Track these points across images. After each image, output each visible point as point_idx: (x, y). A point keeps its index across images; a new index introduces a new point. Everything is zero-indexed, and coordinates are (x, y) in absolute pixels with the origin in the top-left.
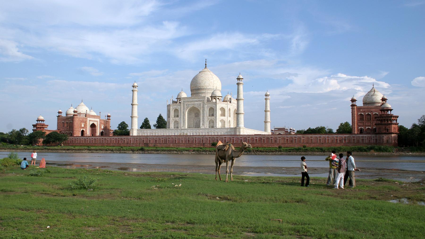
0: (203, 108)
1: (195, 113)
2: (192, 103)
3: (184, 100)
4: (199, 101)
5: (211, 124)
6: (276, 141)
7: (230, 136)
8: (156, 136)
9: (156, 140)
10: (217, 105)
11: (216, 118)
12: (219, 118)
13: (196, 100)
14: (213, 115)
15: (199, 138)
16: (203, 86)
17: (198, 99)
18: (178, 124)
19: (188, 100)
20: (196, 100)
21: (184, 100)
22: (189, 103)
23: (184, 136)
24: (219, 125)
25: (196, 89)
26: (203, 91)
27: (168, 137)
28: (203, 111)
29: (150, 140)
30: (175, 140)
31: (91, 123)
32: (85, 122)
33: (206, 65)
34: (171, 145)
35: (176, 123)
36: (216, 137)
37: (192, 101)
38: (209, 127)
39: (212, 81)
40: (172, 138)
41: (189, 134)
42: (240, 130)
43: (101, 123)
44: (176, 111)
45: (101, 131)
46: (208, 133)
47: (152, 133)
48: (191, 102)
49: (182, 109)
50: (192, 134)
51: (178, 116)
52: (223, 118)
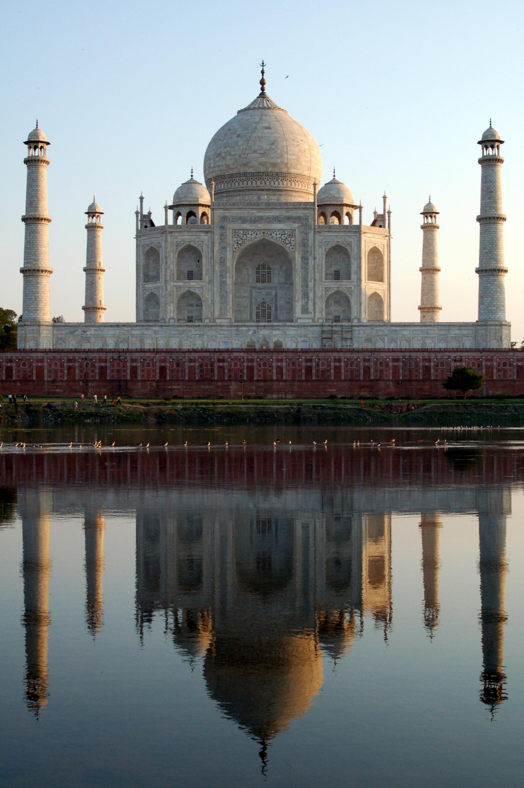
0: (305, 244)
1: (266, 260)
2: (260, 226)
3: (227, 213)
4: (288, 218)
5: (335, 310)
7: (477, 355)
8: (162, 351)
9: (163, 369)
10: (364, 238)
11: (359, 285)
12: (369, 287)
13: (275, 213)
14: (337, 276)
15: (350, 362)
16: (274, 165)
17: (284, 213)
18: (200, 305)
19: (244, 213)
20: (275, 213)
22: (247, 226)
23: (268, 351)
25: (245, 174)
26: (275, 184)
27: (216, 356)
28: (305, 259)
29: (134, 370)
30: (251, 369)
33: (262, 82)
34: (233, 386)
35: (191, 301)
36: (420, 355)
37: (260, 219)
39: (307, 147)
40: (237, 358)
41: (289, 345)
42: (501, 331)
44: (191, 252)
46: (369, 340)
47: (126, 340)
49: (217, 247)
50: (301, 346)
51: (190, 276)
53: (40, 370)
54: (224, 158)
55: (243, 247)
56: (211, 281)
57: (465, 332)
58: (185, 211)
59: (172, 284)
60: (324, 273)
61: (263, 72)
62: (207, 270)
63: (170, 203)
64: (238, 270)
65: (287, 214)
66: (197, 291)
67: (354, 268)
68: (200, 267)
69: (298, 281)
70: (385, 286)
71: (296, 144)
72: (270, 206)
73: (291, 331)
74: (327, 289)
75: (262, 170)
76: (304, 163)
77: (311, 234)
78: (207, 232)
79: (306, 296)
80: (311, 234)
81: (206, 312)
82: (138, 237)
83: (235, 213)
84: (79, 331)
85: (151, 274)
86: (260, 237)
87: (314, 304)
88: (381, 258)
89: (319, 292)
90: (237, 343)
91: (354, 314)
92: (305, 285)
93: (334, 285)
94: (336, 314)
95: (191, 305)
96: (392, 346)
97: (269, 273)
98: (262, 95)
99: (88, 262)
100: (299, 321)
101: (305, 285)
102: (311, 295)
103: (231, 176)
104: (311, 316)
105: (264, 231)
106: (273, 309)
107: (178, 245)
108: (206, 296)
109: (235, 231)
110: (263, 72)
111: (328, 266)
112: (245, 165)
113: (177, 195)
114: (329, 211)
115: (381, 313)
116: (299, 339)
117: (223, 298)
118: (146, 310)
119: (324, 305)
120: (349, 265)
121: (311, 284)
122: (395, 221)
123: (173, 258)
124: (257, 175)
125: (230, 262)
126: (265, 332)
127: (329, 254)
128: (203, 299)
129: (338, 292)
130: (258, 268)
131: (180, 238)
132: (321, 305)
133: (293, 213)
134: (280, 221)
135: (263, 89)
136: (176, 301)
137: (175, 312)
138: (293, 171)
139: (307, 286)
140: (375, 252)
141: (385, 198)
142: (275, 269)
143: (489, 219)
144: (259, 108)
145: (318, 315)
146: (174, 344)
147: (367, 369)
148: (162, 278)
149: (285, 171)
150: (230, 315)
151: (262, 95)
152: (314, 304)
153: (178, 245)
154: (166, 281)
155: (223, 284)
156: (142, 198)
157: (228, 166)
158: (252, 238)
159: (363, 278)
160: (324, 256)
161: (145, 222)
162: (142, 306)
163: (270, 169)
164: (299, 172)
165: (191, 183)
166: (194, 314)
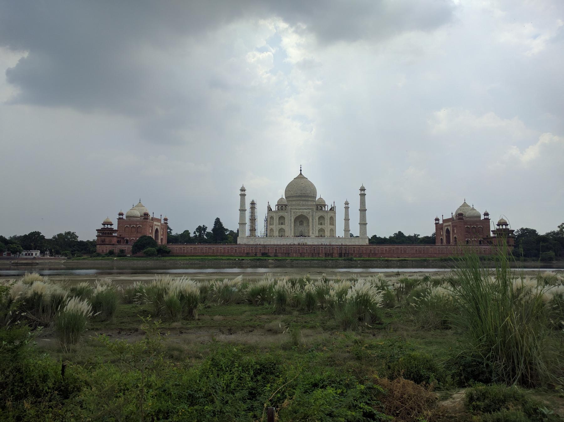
6: (405, 251)
9: (276, 250)
14: (321, 224)
19: (297, 207)
24: (327, 233)
28: (313, 219)
29: (268, 250)
30: (299, 250)
31: (156, 227)
32: (152, 227)
33: (301, 170)
34: (294, 254)
37: (301, 209)
41: (309, 243)
44: (282, 218)
48: (299, 209)
51: (282, 224)
52: (332, 227)
53: (244, 250)
58: (280, 206)
64: (295, 222)
67: (326, 222)
72: (303, 205)
73: (310, 240)
79: (313, 229)
81: (286, 234)
83: (294, 207)
90: (296, 243)
93: (320, 227)
96: (337, 244)
98: (301, 174)
111: (319, 221)
114: (319, 206)
122: (337, 210)
124: (299, 196)
125: (293, 220)
127: (319, 218)
142: (305, 222)
143: (363, 210)
146: (279, 243)
147: (330, 251)
148: (275, 224)
150: (293, 234)
151: (301, 174)
155: (291, 226)
158: (299, 214)
161: (270, 209)
165: (282, 198)
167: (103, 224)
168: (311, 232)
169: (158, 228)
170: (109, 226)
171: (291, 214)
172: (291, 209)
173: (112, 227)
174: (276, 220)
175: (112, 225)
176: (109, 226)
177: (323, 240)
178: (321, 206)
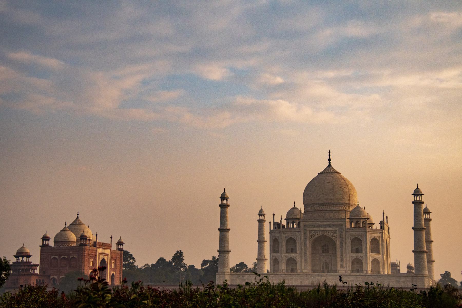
0: (341, 237)
2: (322, 229)
3: (307, 223)
4: (334, 226)
10: (368, 234)
12: (371, 256)
14: (357, 251)
16: (332, 199)
17: (332, 223)
18: (296, 264)
19: (314, 223)
21: (307, 223)
22: (315, 229)
28: (341, 244)
31: (101, 257)
32: (95, 258)
33: (330, 160)
37: (321, 226)
38: (352, 271)
39: (347, 190)
43: (112, 258)
45: (112, 272)
48: (319, 226)
49: (303, 238)
51: (293, 250)
52: (375, 256)
54: (310, 197)
55: (314, 238)
56: (300, 253)
57: (408, 279)
58: (290, 221)
59: (284, 254)
60: (350, 250)
61: (329, 155)
62: (299, 248)
63: (285, 218)
65: (333, 224)
66: (294, 258)
67: (364, 247)
68: (296, 246)
69: (338, 253)
70: (380, 255)
71: (341, 189)
73: (330, 278)
74: (352, 257)
75: (326, 202)
76: (346, 198)
77: (344, 232)
78: (298, 232)
79: (342, 260)
80: (344, 232)
81: (298, 267)
82: (270, 233)
84: (241, 277)
85: (276, 249)
86: (321, 234)
87: (346, 264)
88: (378, 242)
89: (349, 258)
90: (307, 282)
91: (364, 268)
92: (342, 255)
93: (355, 255)
94: (358, 268)
95: (293, 263)
97: (328, 249)
98: (330, 166)
99: (259, 237)
100: (340, 272)
101: (342, 255)
102: (344, 259)
103: (313, 204)
104: (345, 269)
105: (323, 231)
106: (330, 265)
107: (286, 237)
108: (298, 260)
109: (311, 232)
110: (329, 155)
112: (318, 200)
113: (288, 214)
115: (379, 267)
116: (333, 281)
117: (306, 260)
118: (274, 265)
119: (351, 264)
120: (362, 246)
121: (344, 255)
123: (284, 243)
124: (324, 204)
125: (309, 245)
126: (319, 278)
128: (297, 261)
129: (357, 259)
130: (323, 247)
131: (287, 235)
132: (349, 264)
133: (336, 223)
134: (330, 227)
135: (330, 163)
136: (285, 262)
137: (285, 267)
138: (341, 202)
139: (343, 256)
140: (375, 241)
141: (383, 213)
144: (327, 173)
145: (348, 269)
149: (337, 202)
150: (309, 268)
151: (330, 166)
152: (346, 264)
153: (286, 237)
154: (281, 253)
155: (305, 254)
156: (274, 215)
157: (311, 200)
158: (317, 235)
159: (368, 252)
160: (350, 242)
162: (272, 264)
163: (329, 201)
164: (343, 202)
165: (295, 208)
166: (294, 268)
167: (15, 256)
168: (339, 265)
169: (106, 258)
170: (25, 259)
171: (305, 235)
172: (305, 226)
173: (30, 260)
174: (283, 245)
175: (29, 256)
176: (25, 259)
177: (352, 278)
178: (360, 221)
